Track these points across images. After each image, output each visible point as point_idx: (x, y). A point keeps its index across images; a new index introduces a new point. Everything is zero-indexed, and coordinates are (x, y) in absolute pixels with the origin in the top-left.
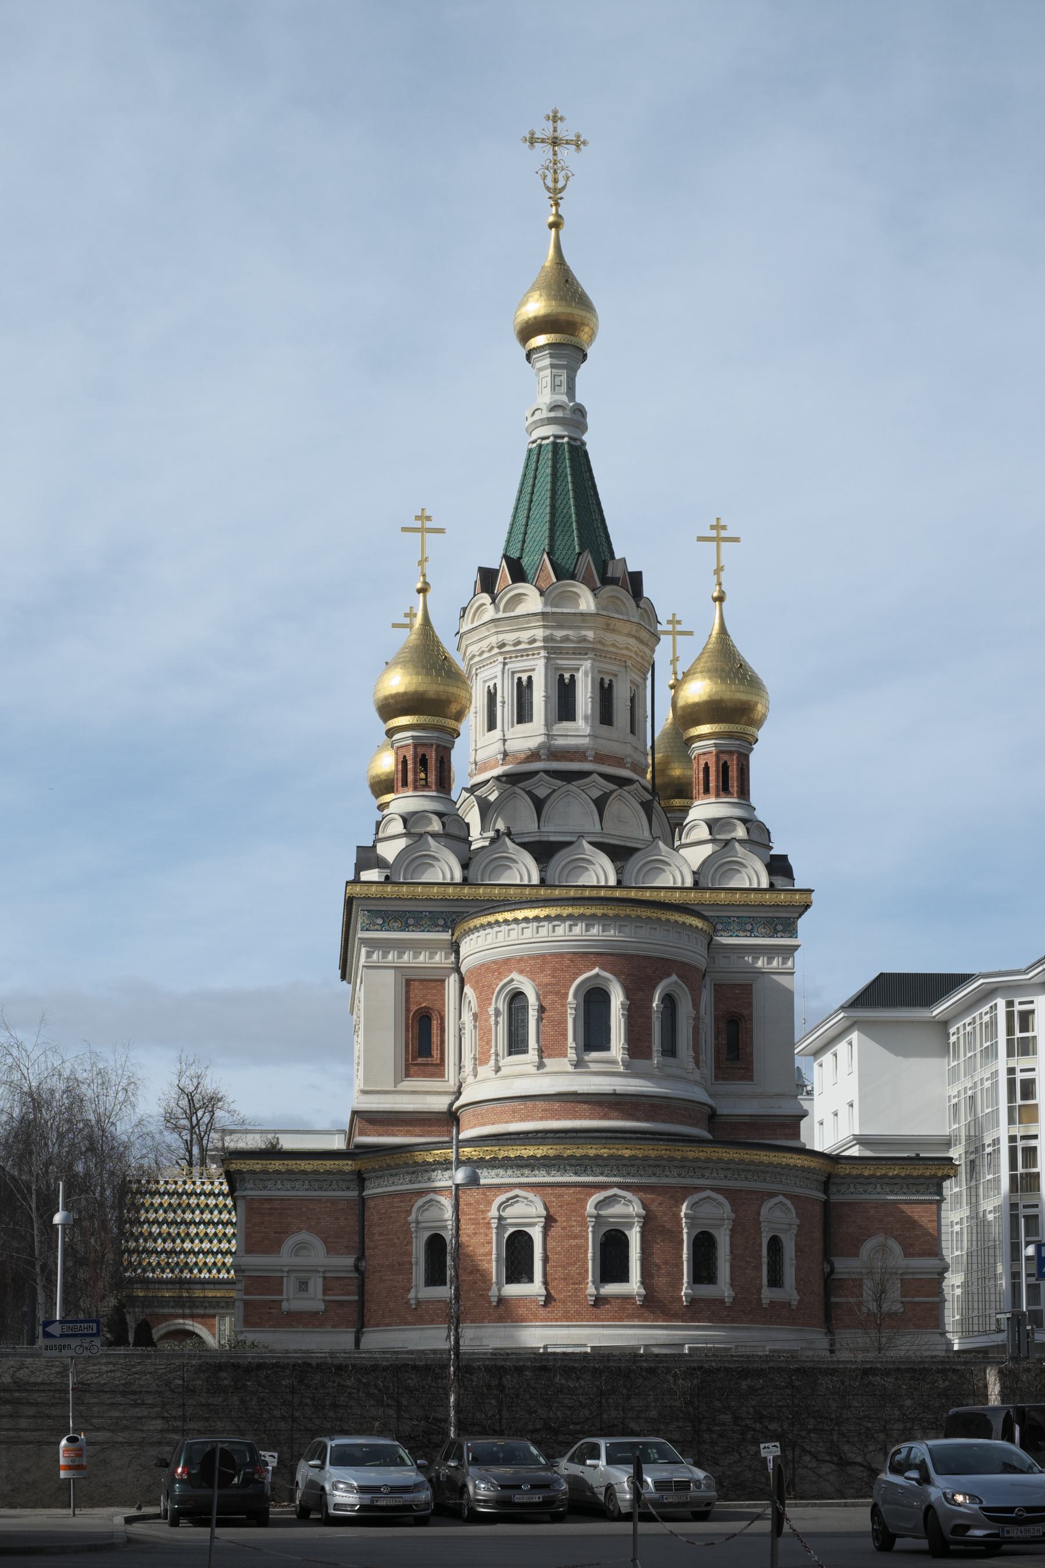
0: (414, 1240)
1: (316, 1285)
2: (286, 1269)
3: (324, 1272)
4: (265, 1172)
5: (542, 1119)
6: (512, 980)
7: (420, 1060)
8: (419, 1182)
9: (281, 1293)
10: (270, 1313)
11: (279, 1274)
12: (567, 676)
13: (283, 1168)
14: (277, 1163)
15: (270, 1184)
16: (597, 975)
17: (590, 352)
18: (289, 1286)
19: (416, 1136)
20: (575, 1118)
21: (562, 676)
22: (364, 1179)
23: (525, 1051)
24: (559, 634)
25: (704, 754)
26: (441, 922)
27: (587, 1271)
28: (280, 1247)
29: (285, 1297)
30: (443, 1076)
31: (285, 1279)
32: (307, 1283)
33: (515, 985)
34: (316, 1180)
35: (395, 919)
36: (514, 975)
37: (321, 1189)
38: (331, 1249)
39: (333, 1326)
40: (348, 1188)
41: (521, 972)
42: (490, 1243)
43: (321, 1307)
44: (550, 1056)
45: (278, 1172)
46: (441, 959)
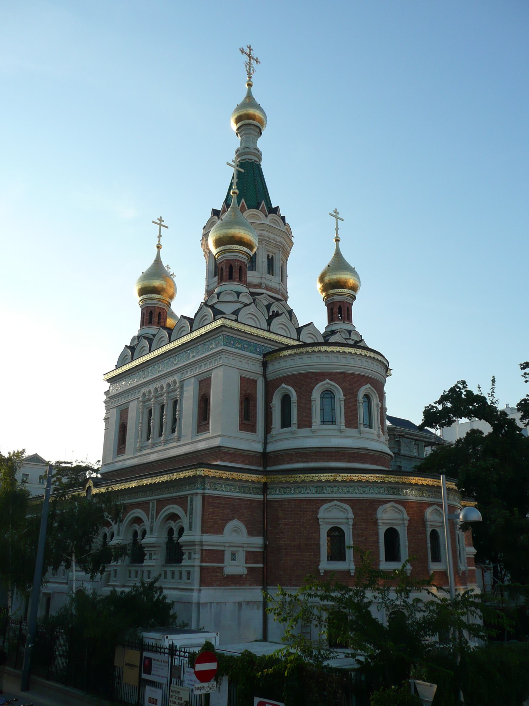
0: (321, 530)
1: (241, 556)
2: (227, 545)
3: (247, 547)
4: (220, 478)
5: (348, 461)
6: (328, 383)
7: (246, 422)
8: (324, 493)
9: (222, 561)
10: (217, 576)
11: (222, 548)
12: (271, 256)
13: (230, 477)
14: (228, 473)
15: (218, 487)
16: (370, 388)
17: (263, 132)
18: (227, 556)
19: (247, 464)
20: (364, 463)
21: (268, 255)
22: (267, 488)
23: (333, 422)
24: (272, 236)
25: (339, 302)
26: (258, 350)
27: (427, 555)
28: (223, 529)
29: (226, 564)
30: (255, 432)
31: (226, 552)
32: (235, 554)
33: (327, 386)
34: (228, 485)
35: (239, 343)
36: (328, 381)
37: (244, 492)
38: (251, 533)
39: (250, 585)
40: (258, 493)
41: (331, 380)
42: (377, 534)
43: (246, 572)
44: (349, 427)
45: (227, 479)
46: (258, 368)
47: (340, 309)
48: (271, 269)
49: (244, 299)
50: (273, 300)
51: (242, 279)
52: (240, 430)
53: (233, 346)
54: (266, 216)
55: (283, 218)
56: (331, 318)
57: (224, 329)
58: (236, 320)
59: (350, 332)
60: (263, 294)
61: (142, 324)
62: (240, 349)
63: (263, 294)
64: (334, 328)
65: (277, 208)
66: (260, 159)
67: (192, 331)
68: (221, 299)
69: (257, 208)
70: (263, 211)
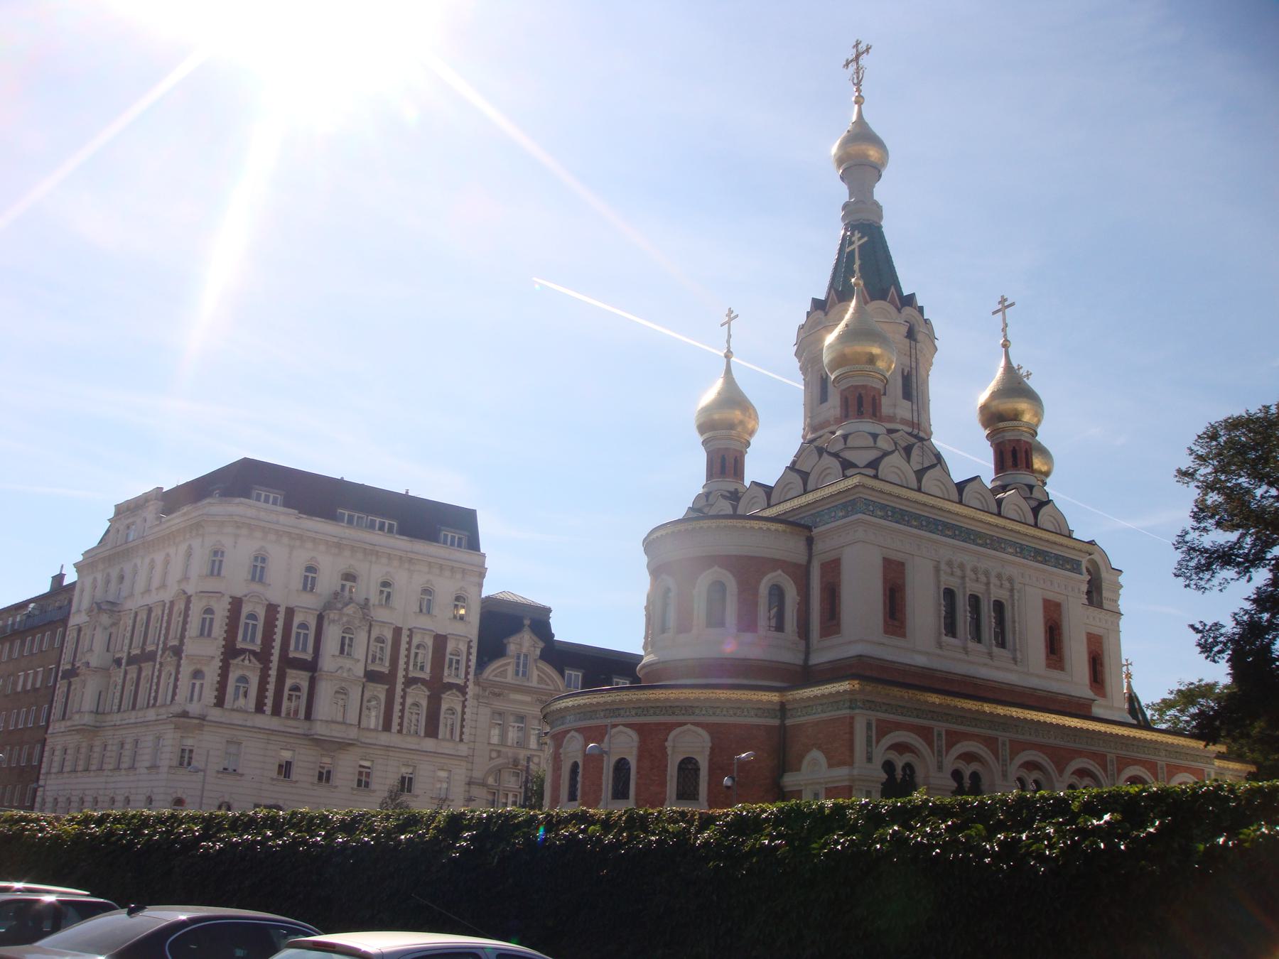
47: (1014, 452)
48: (907, 395)
49: (884, 443)
50: (914, 440)
51: (875, 413)
52: (886, 632)
53: (873, 514)
54: (899, 310)
55: (921, 310)
56: (1000, 466)
57: (861, 489)
58: (876, 477)
59: (1031, 487)
60: (897, 431)
61: (710, 475)
62: (881, 517)
63: (897, 431)
64: (1008, 480)
65: (912, 296)
66: (881, 217)
67: (805, 492)
68: (850, 443)
69: (884, 298)
70: (892, 302)
